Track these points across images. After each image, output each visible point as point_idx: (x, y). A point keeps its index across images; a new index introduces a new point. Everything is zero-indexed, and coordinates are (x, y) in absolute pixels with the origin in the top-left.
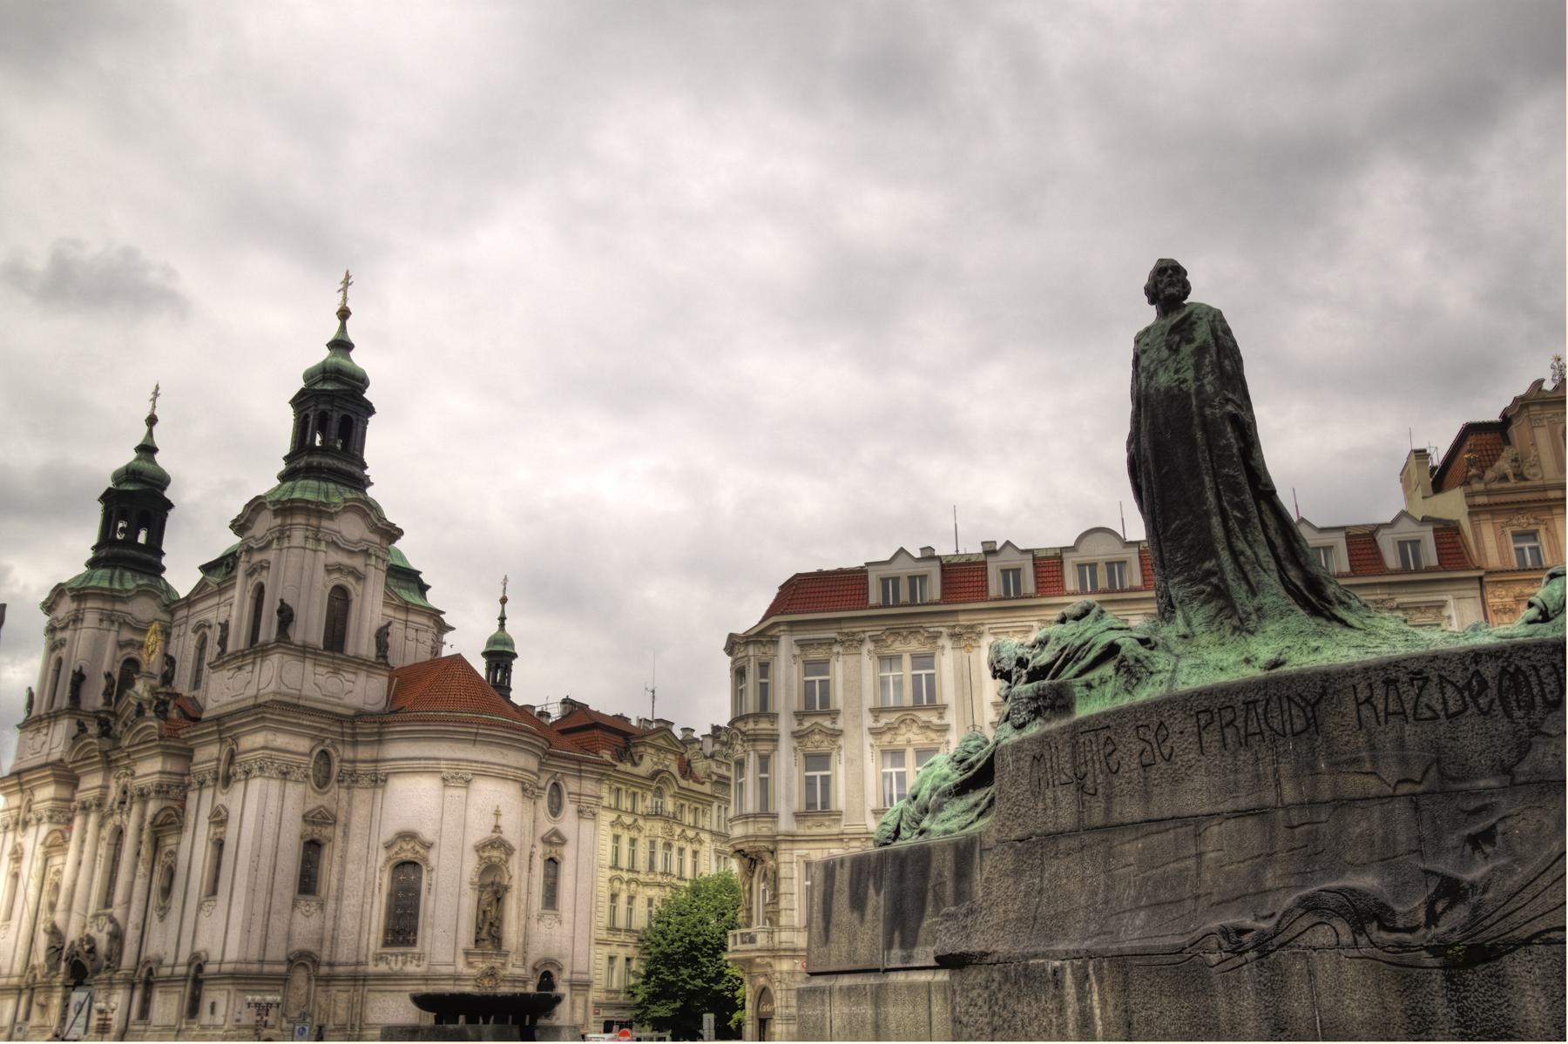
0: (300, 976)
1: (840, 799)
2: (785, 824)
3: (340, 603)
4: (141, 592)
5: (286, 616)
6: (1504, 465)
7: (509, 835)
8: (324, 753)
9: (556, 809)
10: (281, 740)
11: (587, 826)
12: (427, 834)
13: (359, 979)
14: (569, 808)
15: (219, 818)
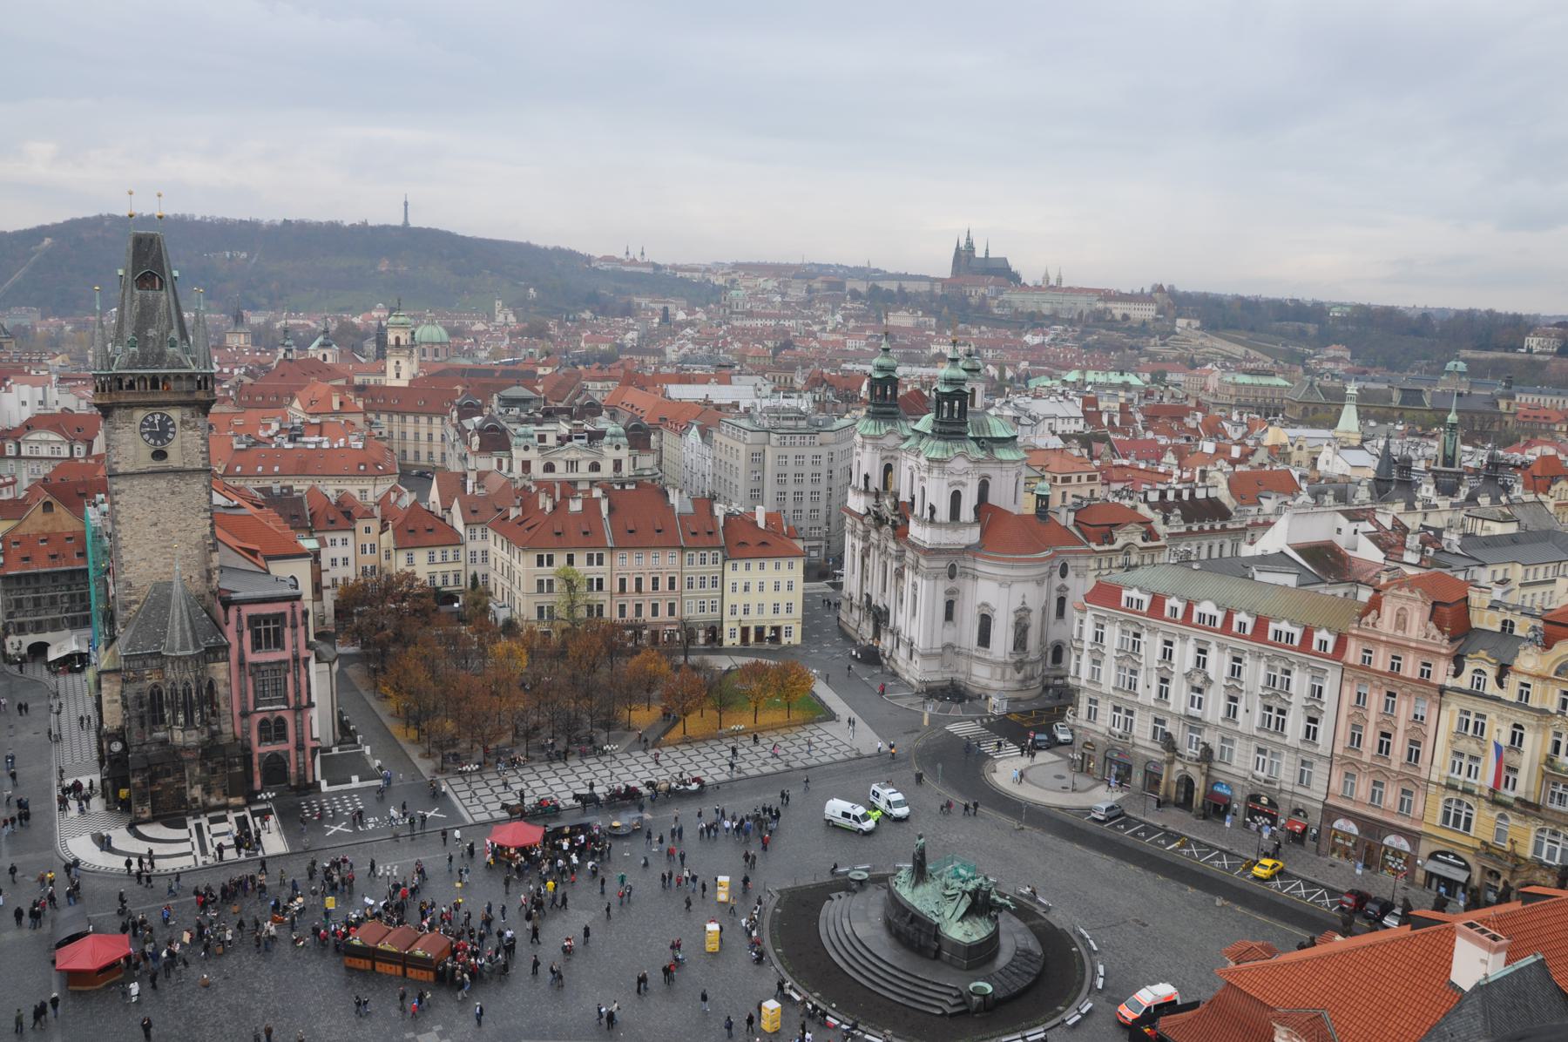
0: (948, 651)
1: (1102, 681)
2: (1083, 683)
3: (956, 498)
4: (889, 433)
5: (932, 509)
6: (1370, 619)
7: (1029, 605)
8: (953, 566)
9: (1063, 574)
10: (934, 564)
11: (1081, 581)
12: (993, 605)
13: (970, 657)
14: (1071, 574)
15: (914, 585)
